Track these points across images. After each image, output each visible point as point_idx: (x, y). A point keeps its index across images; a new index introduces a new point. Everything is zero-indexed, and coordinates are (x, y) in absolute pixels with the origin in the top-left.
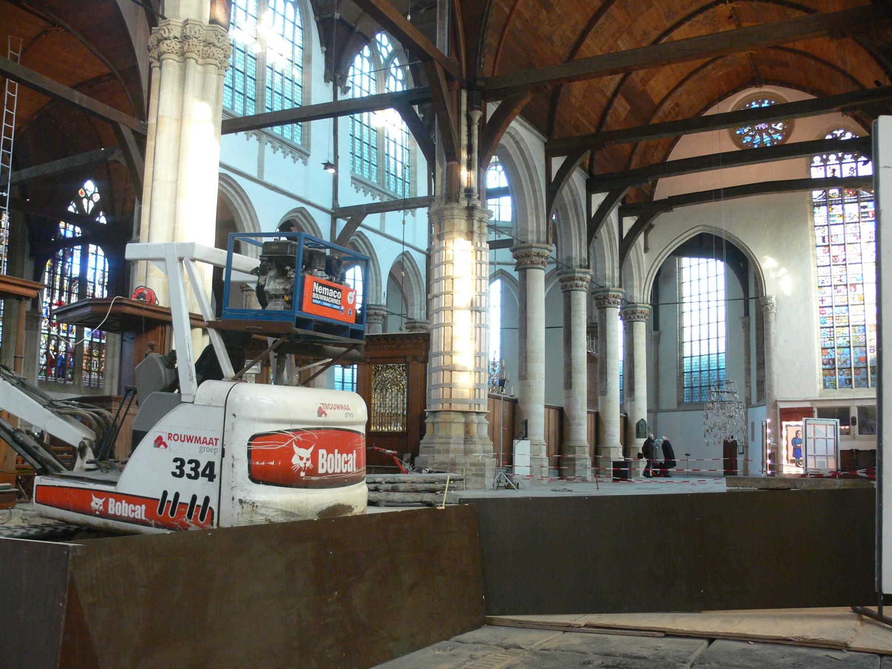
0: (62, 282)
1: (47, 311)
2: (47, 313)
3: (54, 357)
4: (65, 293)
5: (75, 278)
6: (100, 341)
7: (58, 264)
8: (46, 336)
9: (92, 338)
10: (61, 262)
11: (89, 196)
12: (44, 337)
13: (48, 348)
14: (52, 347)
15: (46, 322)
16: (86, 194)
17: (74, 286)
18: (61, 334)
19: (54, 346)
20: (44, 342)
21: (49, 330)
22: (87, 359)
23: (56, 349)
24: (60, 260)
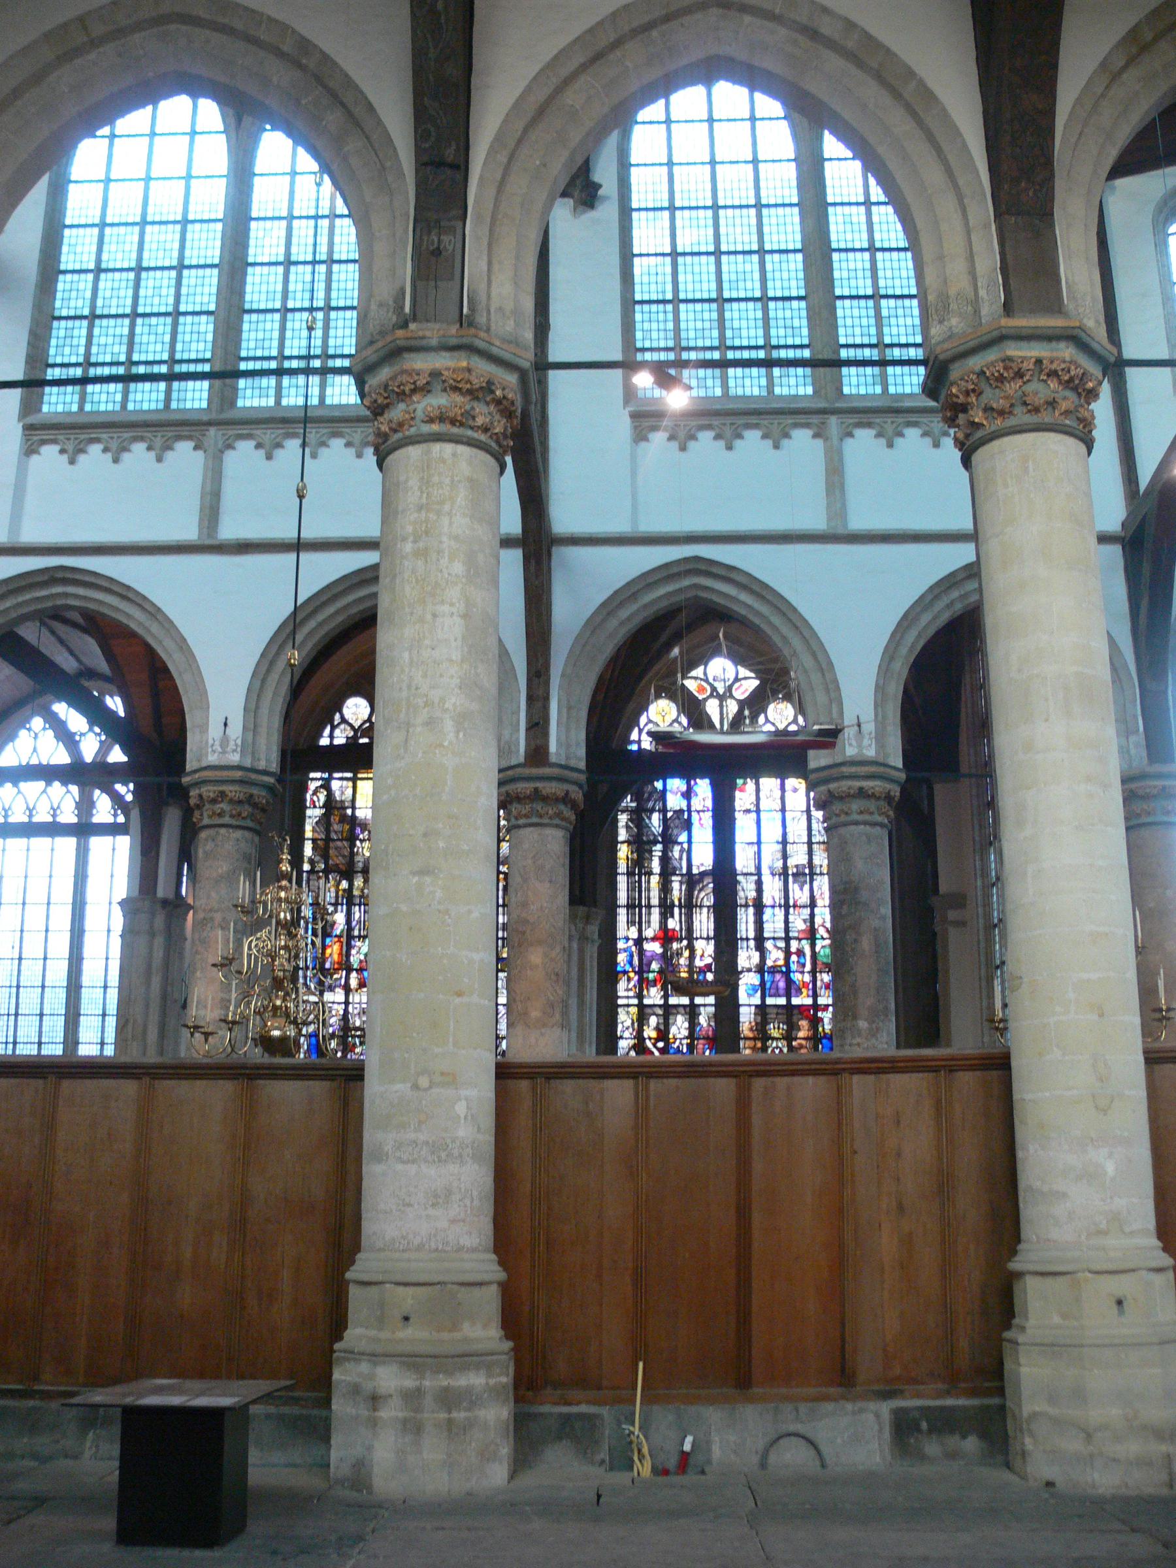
0: (665, 888)
1: (631, 956)
2: (631, 963)
4: (676, 910)
5: (703, 874)
6: (789, 1000)
7: (651, 851)
8: (634, 1010)
9: (763, 998)
10: (659, 847)
12: (628, 1013)
13: (640, 1037)
14: (650, 1032)
15: (629, 980)
16: (714, 689)
17: (701, 890)
19: (657, 1029)
20: (629, 1023)
21: (640, 996)
23: (663, 1034)
24: (655, 842)
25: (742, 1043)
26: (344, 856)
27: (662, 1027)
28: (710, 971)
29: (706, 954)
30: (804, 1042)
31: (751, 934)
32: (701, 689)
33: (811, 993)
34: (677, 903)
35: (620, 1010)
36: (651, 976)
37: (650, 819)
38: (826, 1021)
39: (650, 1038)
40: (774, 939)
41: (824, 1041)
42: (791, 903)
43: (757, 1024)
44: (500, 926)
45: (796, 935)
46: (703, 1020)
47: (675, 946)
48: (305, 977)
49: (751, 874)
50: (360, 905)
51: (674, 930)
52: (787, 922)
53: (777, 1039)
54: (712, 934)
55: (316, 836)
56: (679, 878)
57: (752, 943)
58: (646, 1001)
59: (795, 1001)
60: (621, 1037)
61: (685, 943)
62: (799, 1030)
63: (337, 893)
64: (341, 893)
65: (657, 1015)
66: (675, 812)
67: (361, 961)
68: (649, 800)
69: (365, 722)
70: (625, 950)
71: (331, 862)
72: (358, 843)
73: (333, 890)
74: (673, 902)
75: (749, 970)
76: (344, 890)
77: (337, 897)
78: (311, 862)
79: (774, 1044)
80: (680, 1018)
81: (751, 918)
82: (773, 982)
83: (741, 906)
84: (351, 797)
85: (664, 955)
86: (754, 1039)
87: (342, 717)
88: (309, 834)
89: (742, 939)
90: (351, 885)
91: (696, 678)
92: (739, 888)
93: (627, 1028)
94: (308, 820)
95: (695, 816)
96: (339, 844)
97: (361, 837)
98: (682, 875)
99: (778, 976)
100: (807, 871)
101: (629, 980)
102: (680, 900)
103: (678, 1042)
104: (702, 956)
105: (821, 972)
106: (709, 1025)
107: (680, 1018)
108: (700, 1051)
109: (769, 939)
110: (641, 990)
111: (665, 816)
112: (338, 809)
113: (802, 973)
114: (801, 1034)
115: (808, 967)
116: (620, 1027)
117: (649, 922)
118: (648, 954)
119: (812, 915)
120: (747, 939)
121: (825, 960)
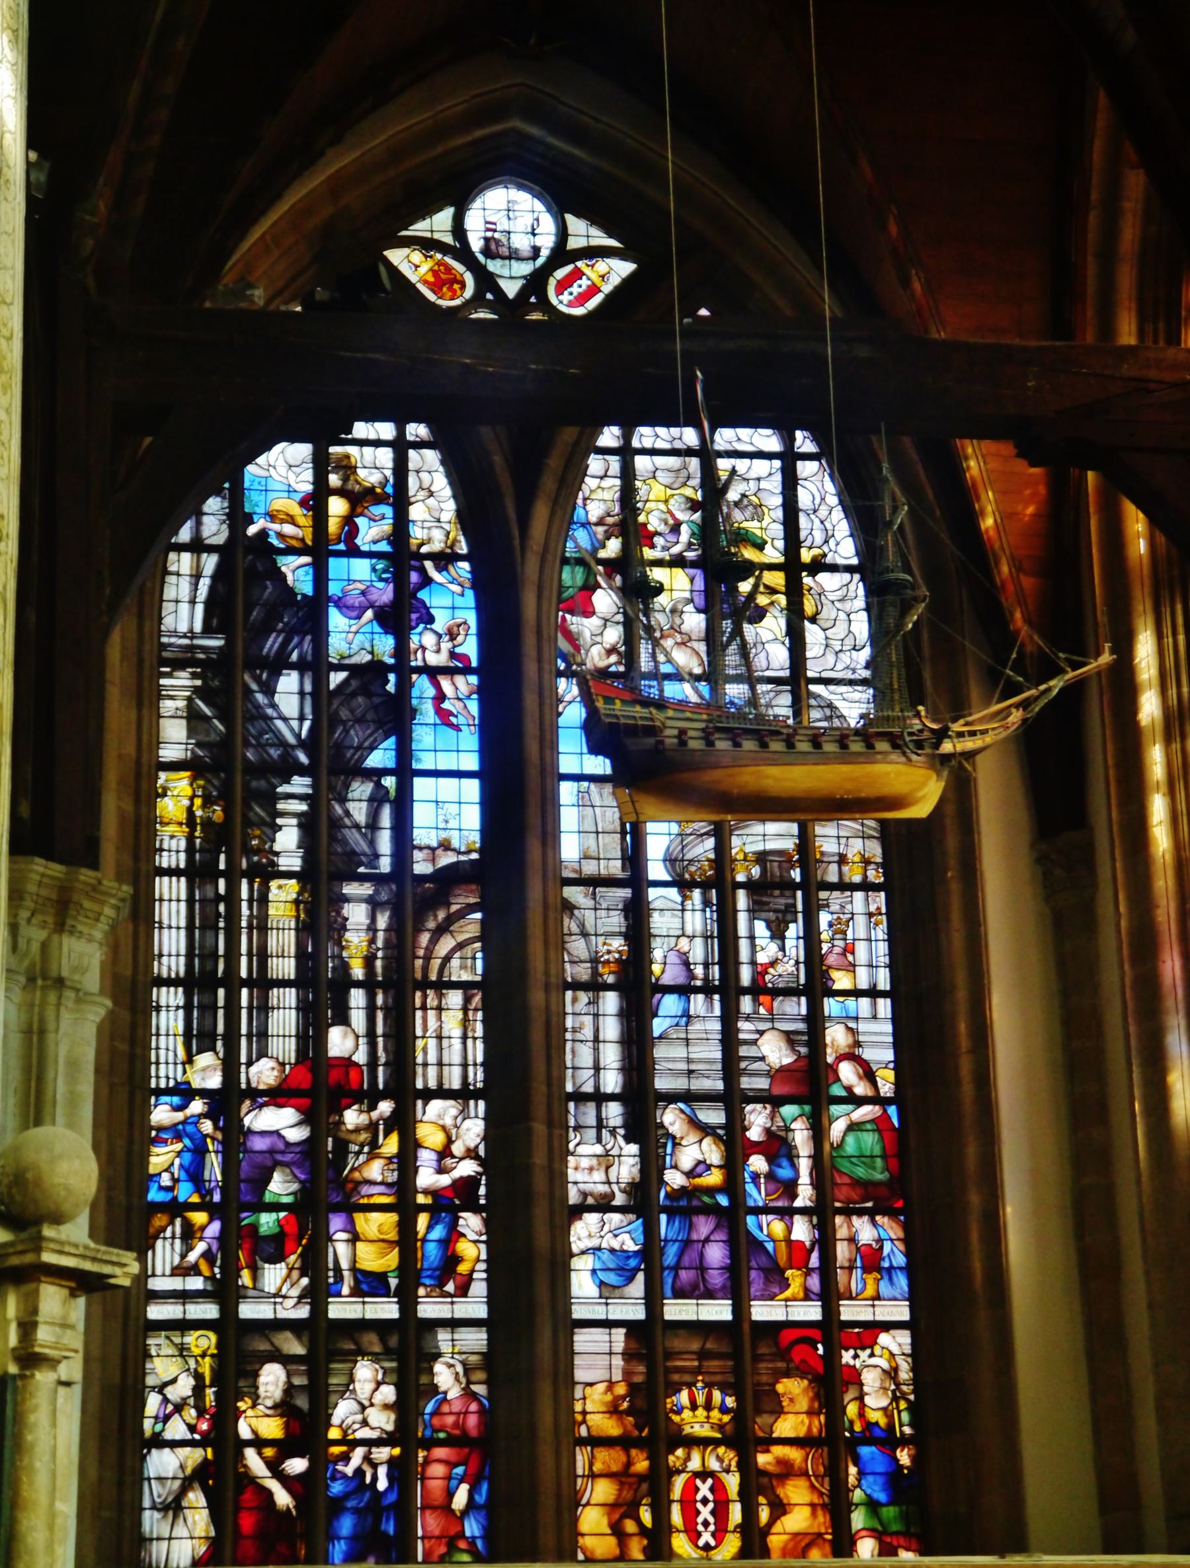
1: (199, 1151)
2: (195, 1174)
3: (283, 1498)
4: (357, 998)
5: (448, 879)
7: (270, 799)
8: (202, 1342)
9: (653, 1300)
10: (300, 784)
11: (511, 289)
12: (182, 1351)
15: (189, 1234)
17: (442, 930)
18: (341, 1309)
20: (184, 1387)
22: (621, 1476)
24: (289, 769)
25: (581, 1458)
27: (302, 1402)
28: (476, 1209)
29: (458, 1149)
30: (794, 1454)
31: (612, 1082)
32: (443, 281)
33: (814, 1282)
34: (358, 972)
35: (155, 1342)
36: (267, 1222)
37: (270, 691)
38: (871, 1379)
39: (258, 1443)
40: (689, 1097)
41: (865, 1451)
42: (746, 976)
43: (633, 1389)
45: (763, 1083)
46: (444, 1376)
47: (352, 1117)
49: (610, 882)
51: (347, 1063)
52: (729, 1040)
53: (704, 1442)
54: (477, 1077)
56: (366, 889)
57: (614, 1112)
58: (248, 1311)
59: (762, 1311)
60: (158, 1442)
61: (385, 1107)
62: (779, 1411)
65: (285, 1360)
66: (355, 670)
68: (266, 629)
70: (176, 1130)
74: (344, 967)
75: (604, 1205)
79: (695, 1464)
80: (365, 1372)
81: (611, 1029)
82: (687, 1244)
83: (577, 986)
85: (309, 1147)
86: (623, 1442)
89: (580, 1097)
91: (428, 245)
92: (571, 925)
93: (179, 1408)
95: (422, 687)
98: (378, 879)
99: (704, 1226)
100: (796, 875)
101: (189, 1234)
102: (369, 961)
103: (358, 1454)
104: (445, 1153)
105: (848, 1212)
106: (469, 1395)
107: (365, 1372)
108: (436, 1486)
109: (671, 1098)
110: (231, 1271)
111: (320, 682)
113: (787, 1214)
114: (786, 1427)
115: (805, 1195)
116: (153, 1403)
117: (263, 1035)
118: (259, 1144)
119: (815, 1021)
120: (599, 1098)
121: (861, 1172)
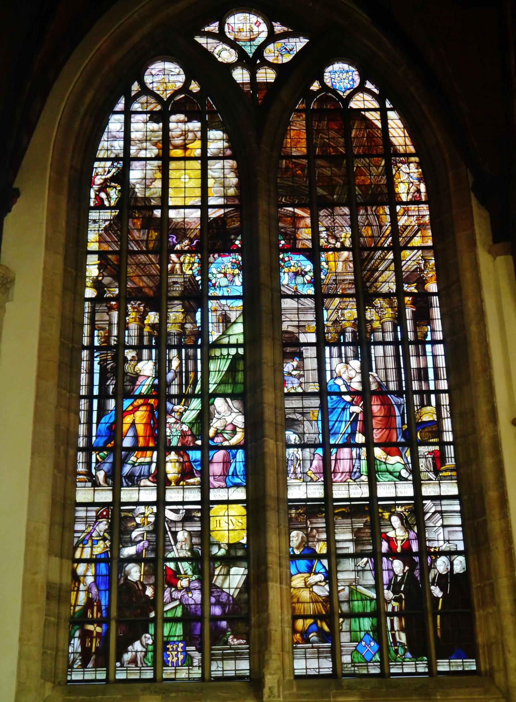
26: (150, 276)
44: (414, 373)
48: (88, 463)
50: (179, 347)
55: (105, 247)
63: (141, 329)
64: (147, 329)
67: (183, 435)
69: (176, 93)
71: (130, 285)
72: (173, 257)
73: (133, 326)
76: (153, 326)
77: (141, 336)
78: (98, 284)
84: (158, 192)
87: (142, 84)
88: (93, 246)
90: (164, 318)
94: (92, 226)
96: (143, 258)
97: (178, 247)
112: (139, 209)
